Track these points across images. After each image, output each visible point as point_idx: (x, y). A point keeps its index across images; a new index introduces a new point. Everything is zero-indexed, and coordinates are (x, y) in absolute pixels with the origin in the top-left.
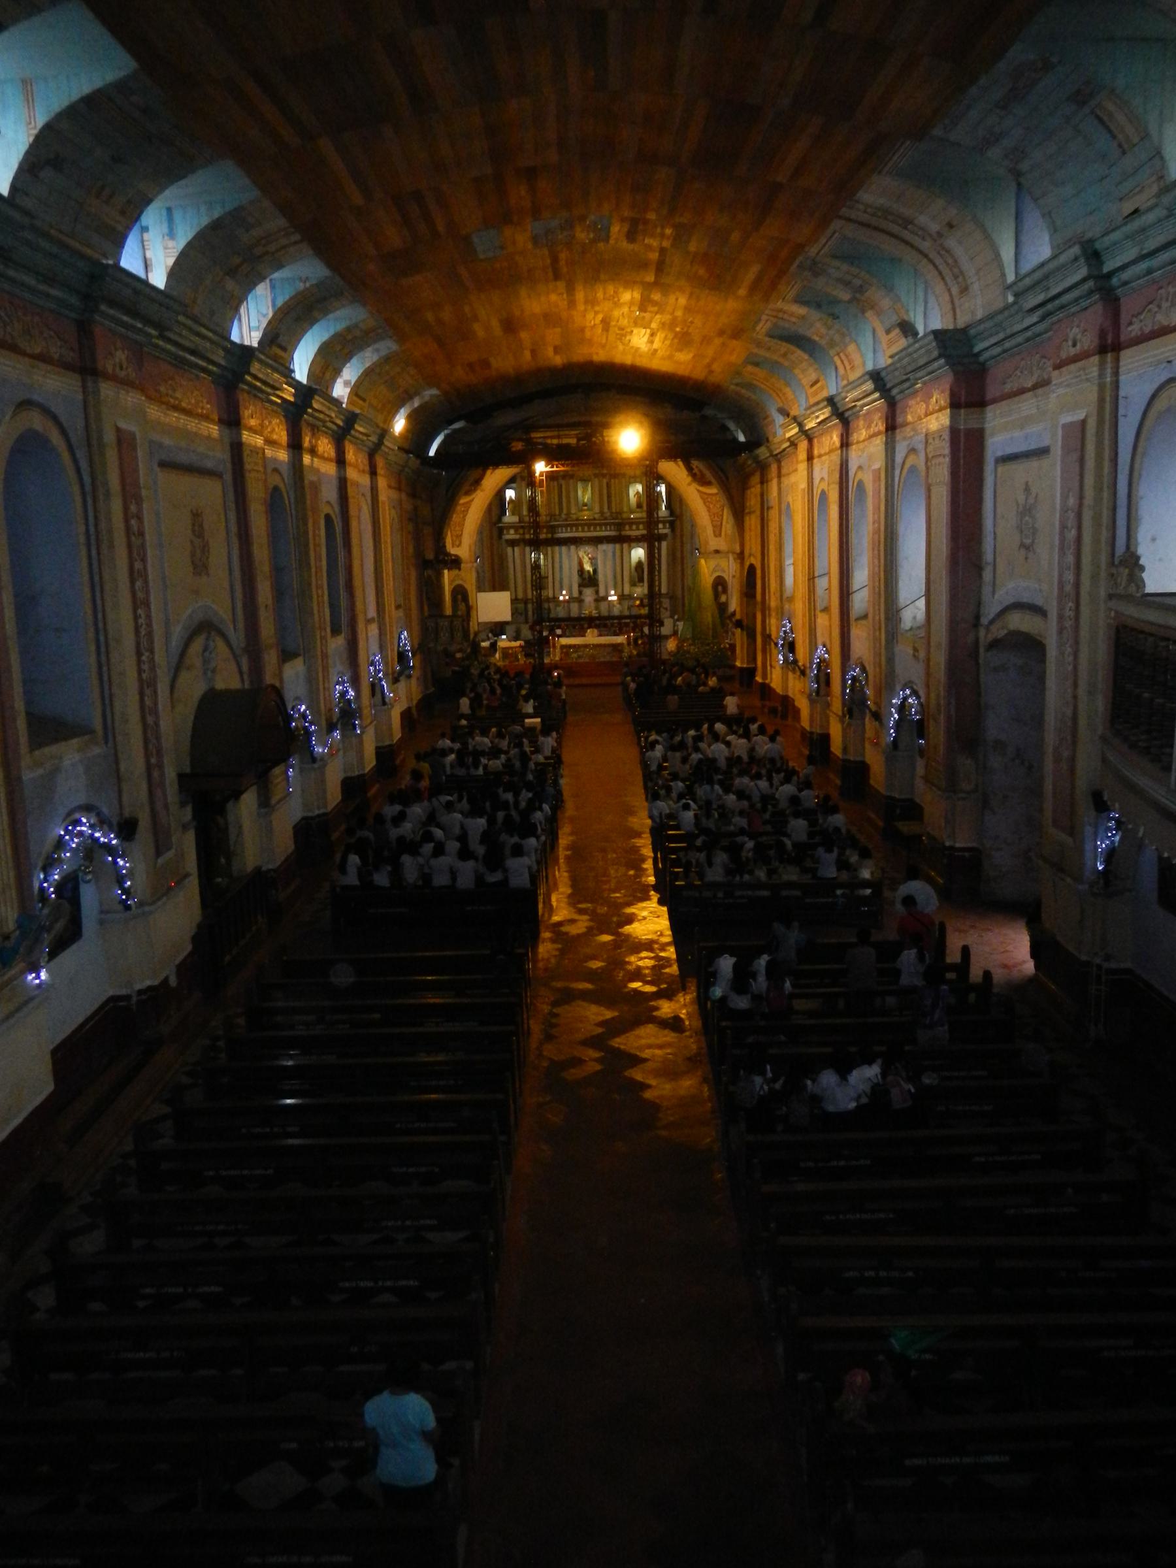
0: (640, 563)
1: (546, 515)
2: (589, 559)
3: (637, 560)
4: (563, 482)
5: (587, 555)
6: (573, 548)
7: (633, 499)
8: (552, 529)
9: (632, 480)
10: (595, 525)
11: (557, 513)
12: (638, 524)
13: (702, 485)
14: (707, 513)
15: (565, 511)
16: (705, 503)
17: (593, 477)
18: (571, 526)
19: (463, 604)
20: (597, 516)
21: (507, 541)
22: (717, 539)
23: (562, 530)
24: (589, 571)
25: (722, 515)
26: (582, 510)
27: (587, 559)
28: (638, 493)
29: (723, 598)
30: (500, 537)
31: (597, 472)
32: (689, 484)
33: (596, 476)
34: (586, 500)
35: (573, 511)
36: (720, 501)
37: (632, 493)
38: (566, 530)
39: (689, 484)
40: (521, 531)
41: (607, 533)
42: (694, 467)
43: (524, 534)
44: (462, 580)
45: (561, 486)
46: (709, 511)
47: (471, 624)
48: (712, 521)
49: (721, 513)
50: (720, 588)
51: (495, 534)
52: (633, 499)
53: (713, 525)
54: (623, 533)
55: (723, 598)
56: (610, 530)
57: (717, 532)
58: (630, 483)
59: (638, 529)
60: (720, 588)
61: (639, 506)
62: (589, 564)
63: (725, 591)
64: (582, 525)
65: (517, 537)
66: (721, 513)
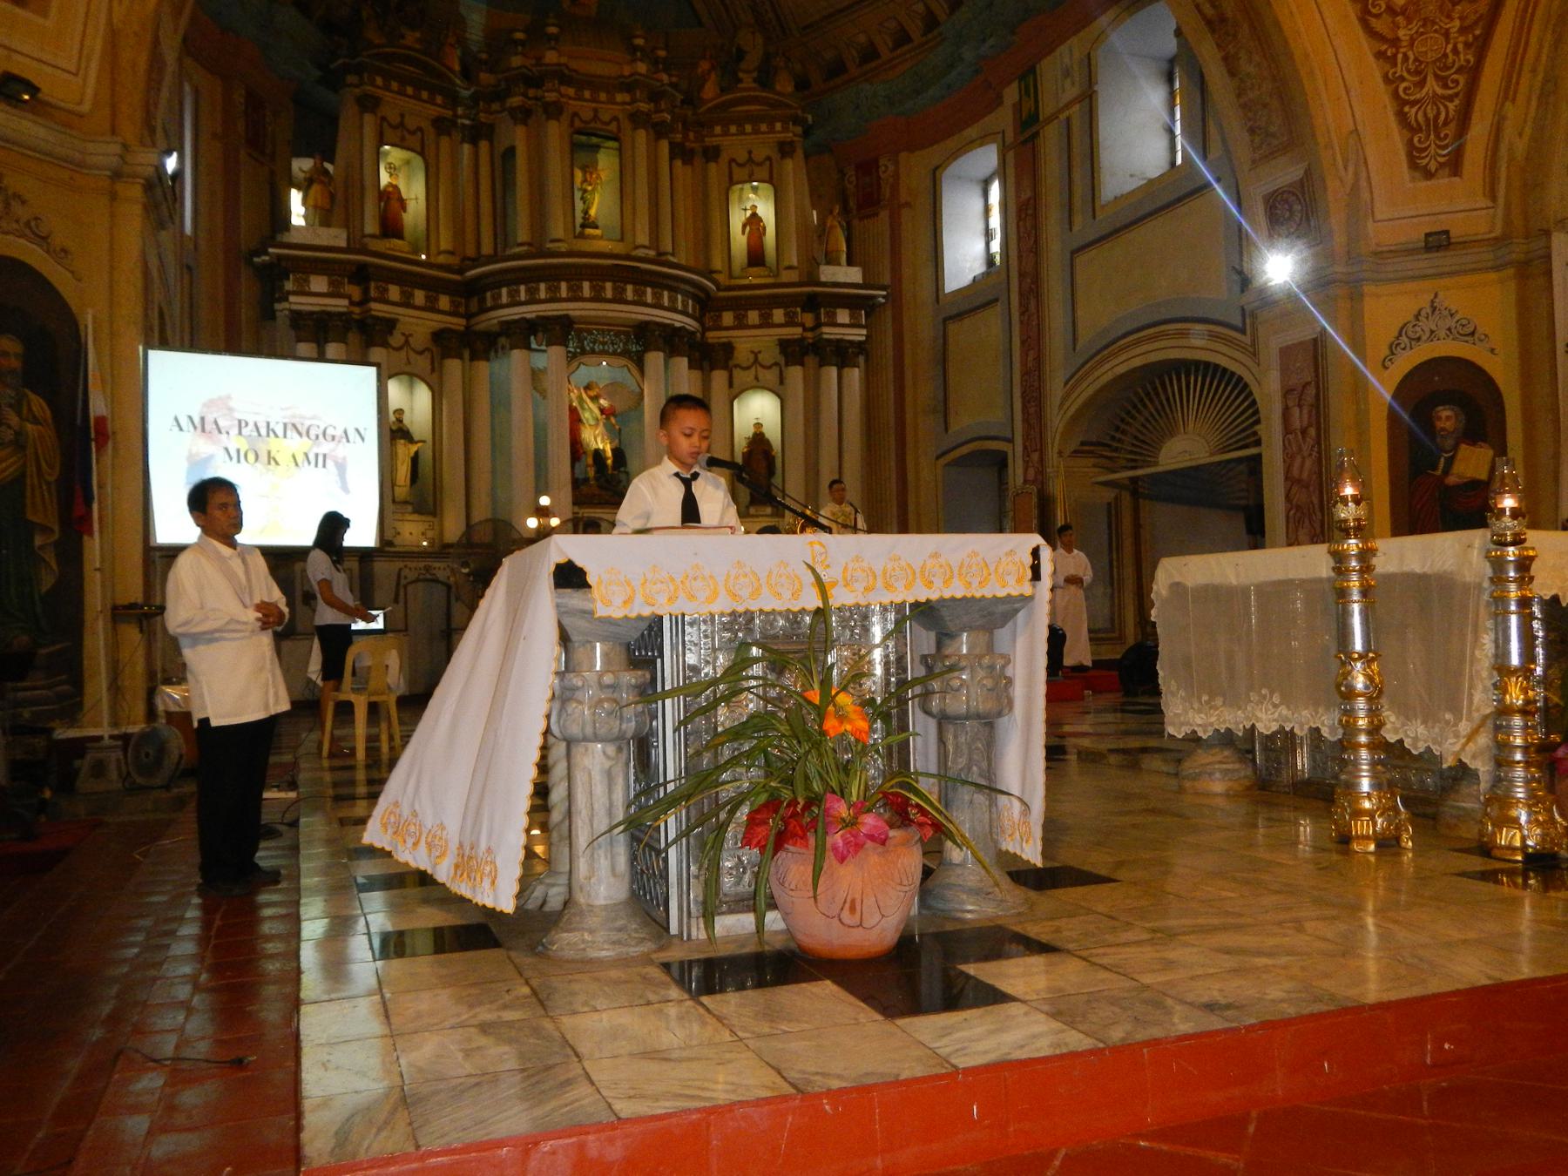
0: (758, 440)
1: (451, 253)
2: (602, 411)
3: (750, 432)
4: (519, 137)
5: (595, 399)
6: (549, 358)
7: (739, 240)
8: (471, 293)
9: (738, 173)
10: (642, 279)
11: (487, 249)
12: (766, 304)
14: (1375, 70)
15: (523, 235)
17: (626, 125)
18: (552, 275)
19: (38, 404)
20: (641, 253)
21: (297, 318)
22: (1443, 181)
23: (513, 294)
24: (598, 454)
25: (1474, 73)
26: (582, 236)
27: (597, 412)
28: (754, 220)
30: (270, 315)
31: (644, 107)
33: (637, 120)
34: (593, 212)
35: (557, 229)
37: (737, 219)
38: (532, 292)
40: (355, 292)
41: (678, 320)
43: (365, 300)
44: (43, 240)
45: (510, 152)
46: (1387, 49)
47: (94, 548)
48: (1401, 103)
50: (1447, 418)
51: (248, 289)
52: (739, 240)
53: (1402, 117)
54: (713, 336)
56: (684, 313)
57: (1436, 155)
58: (732, 182)
59: (766, 323)
60: (1447, 418)
61: (756, 256)
62: (600, 429)
64: (597, 275)
65: (339, 305)
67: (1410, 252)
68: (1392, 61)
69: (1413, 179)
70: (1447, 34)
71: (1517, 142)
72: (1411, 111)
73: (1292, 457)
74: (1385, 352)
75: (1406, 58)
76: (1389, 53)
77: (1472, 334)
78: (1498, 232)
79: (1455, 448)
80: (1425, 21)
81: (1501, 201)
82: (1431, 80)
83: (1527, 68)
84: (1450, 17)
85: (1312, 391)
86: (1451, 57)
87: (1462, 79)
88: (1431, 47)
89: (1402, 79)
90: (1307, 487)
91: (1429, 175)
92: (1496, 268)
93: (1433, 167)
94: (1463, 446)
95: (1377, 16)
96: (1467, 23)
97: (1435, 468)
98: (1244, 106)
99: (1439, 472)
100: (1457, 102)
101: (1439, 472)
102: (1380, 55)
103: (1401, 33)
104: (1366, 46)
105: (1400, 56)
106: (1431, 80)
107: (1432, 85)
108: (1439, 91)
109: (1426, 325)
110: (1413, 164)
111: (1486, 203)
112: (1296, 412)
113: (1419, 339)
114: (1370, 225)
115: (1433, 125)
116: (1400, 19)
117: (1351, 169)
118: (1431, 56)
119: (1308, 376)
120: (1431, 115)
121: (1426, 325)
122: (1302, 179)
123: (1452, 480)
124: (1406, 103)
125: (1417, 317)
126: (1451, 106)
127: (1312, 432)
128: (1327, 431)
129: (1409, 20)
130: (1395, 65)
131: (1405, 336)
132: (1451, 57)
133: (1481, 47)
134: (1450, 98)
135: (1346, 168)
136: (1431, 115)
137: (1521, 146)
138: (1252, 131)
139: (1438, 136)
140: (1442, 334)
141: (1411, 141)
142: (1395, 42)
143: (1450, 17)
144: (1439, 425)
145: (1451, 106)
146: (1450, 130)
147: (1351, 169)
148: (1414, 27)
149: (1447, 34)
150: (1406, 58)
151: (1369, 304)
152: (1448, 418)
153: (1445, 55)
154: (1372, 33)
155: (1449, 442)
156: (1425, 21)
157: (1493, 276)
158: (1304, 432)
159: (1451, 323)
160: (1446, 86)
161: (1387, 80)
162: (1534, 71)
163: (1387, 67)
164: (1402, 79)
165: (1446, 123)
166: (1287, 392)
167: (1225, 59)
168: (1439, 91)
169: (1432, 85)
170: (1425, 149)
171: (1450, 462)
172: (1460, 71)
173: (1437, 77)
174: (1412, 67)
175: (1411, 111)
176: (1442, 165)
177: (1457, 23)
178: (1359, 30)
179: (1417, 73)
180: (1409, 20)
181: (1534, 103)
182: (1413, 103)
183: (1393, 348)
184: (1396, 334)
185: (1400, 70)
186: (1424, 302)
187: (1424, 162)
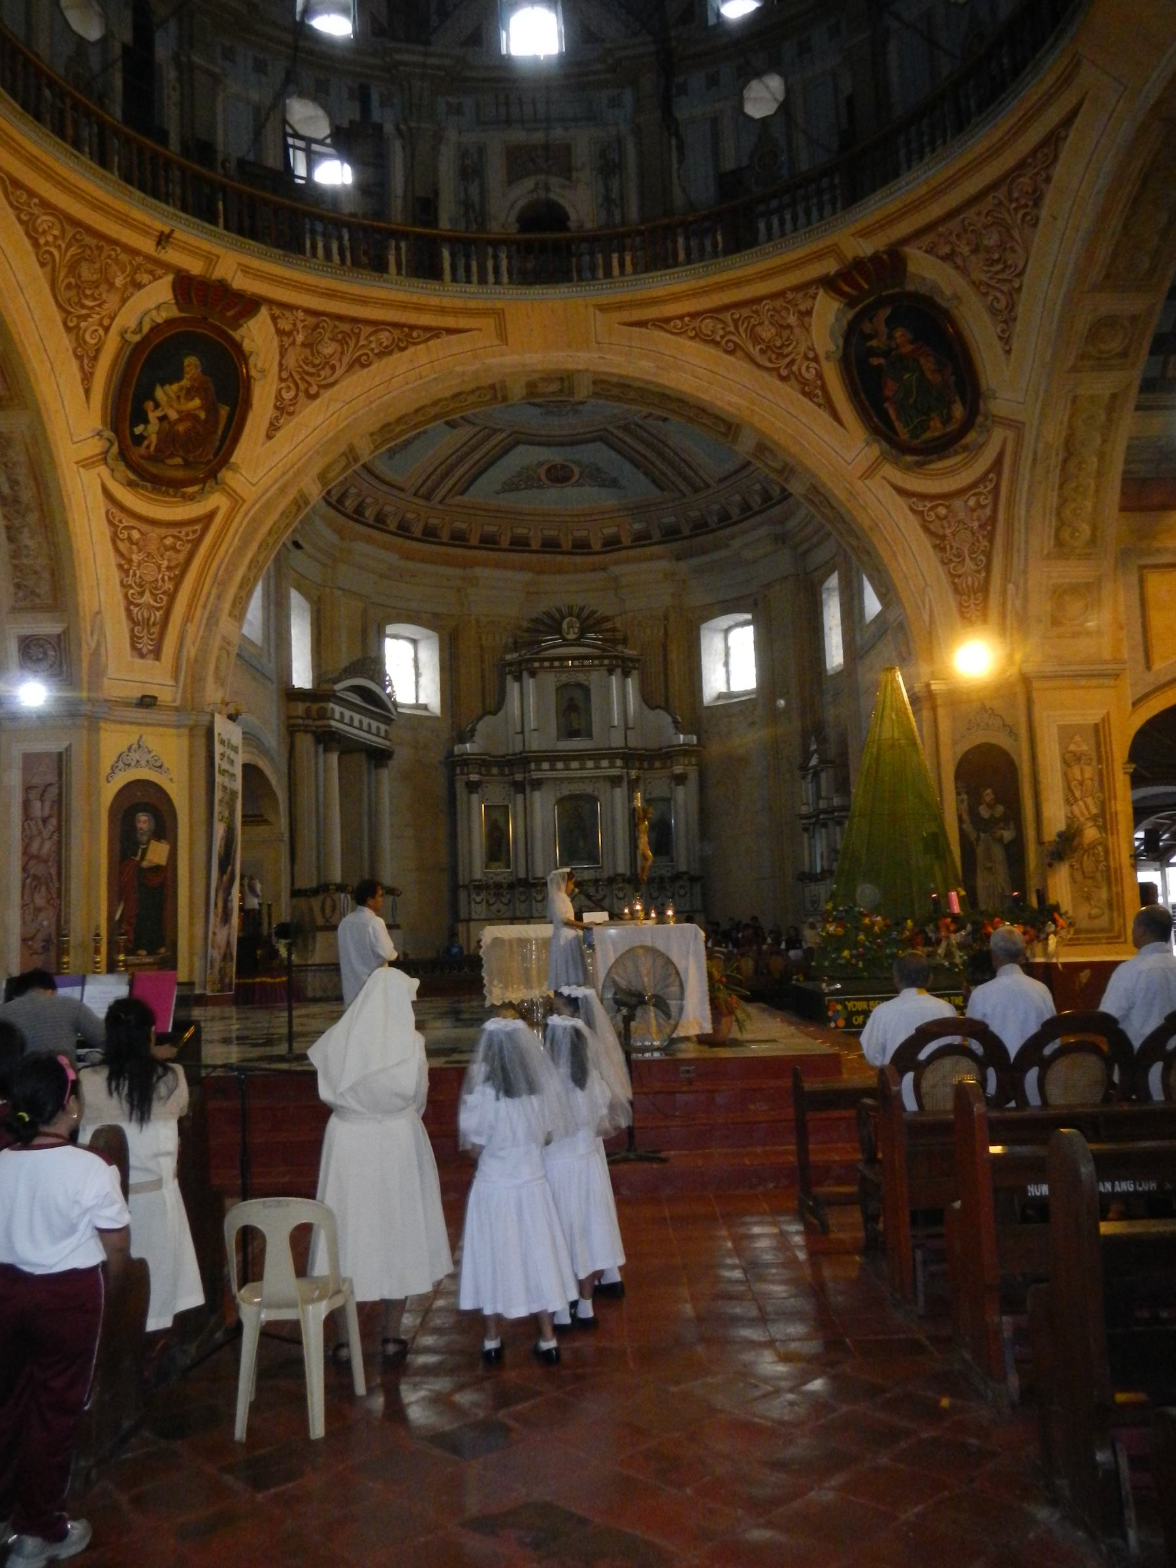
13: (131, 484)
16: (114, 539)
22: (149, 662)
25: (172, 597)
29: (157, 854)
32: (86, 463)
36: (173, 548)
39: (86, 463)
42: (153, 416)
49: (169, 586)
50: (144, 821)
53: (129, 612)
55: (157, 854)
57: (146, 645)
60: (144, 821)
63: (165, 829)
66: (169, 586)
67: (126, 704)
68: (127, 572)
69: (132, 656)
70: (159, 567)
71: (191, 650)
72: (135, 610)
73: (31, 838)
74: (109, 770)
75: (135, 575)
76: (126, 567)
77: (160, 767)
78: (177, 704)
79: (148, 842)
80: (149, 555)
81: (181, 684)
82: (147, 594)
83: (201, 603)
84: (162, 556)
85: (54, 791)
86: (160, 583)
87: (165, 598)
88: (149, 572)
89: (131, 587)
90: (46, 862)
91: (142, 656)
92: (178, 727)
93: (145, 651)
94: (153, 842)
95: (122, 540)
96: (173, 564)
97: (136, 855)
98: (15, 566)
99: (138, 858)
100: (161, 612)
101: (138, 858)
102: (120, 566)
103: (134, 557)
104: (113, 559)
105: (131, 572)
106: (147, 594)
107: (147, 598)
108: (152, 602)
109: (135, 756)
110: (133, 647)
111: (171, 682)
112: (38, 804)
113: (129, 765)
114: (105, 680)
115: (147, 623)
116: (134, 547)
117: (95, 637)
118: (149, 578)
119: (51, 778)
120: (146, 616)
121: (135, 756)
122: (59, 636)
123: (145, 864)
124: (132, 603)
125: (130, 749)
126: (158, 614)
127: (54, 821)
128: (68, 821)
129: (140, 551)
130: (128, 576)
131: (122, 761)
132: (160, 583)
133: (178, 581)
134: (158, 609)
135: (92, 634)
136: (146, 616)
137: (193, 652)
138: (18, 586)
139: (149, 631)
140: (143, 763)
141: (132, 630)
142: (130, 561)
143: (162, 556)
144: (140, 825)
145: (158, 614)
146: (155, 630)
147: (95, 637)
148: (142, 556)
149: (159, 567)
150: (135, 575)
151: (103, 735)
152: (145, 822)
153: (157, 580)
154: (117, 550)
155: (145, 839)
156: (149, 555)
157: (174, 731)
158: (45, 820)
159: (149, 757)
160: (156, 601)
161: (121, 581)
162: (205, 607)
163: (123, 576)
164: (131, 587)
165: (154, 624)
166: (28, 789)
167: (8, 528)
168: (152, 602)
169: (147, 598)
170: (141, 638)
171: (145, 851)
172: (164, 593)
173: (151, 593)
174: (138, 581)
175: (135, 610)
176: (150, 651)
177: (165, 563)
178: (110, 545)
179: (141, 586)
180: (140, 551)
181: (203, 627)
182: (137, 605)
183: (114, 769)
184: (115, 759)
185: (130, 581)
186: (134, 739)
187: (140, 646)
